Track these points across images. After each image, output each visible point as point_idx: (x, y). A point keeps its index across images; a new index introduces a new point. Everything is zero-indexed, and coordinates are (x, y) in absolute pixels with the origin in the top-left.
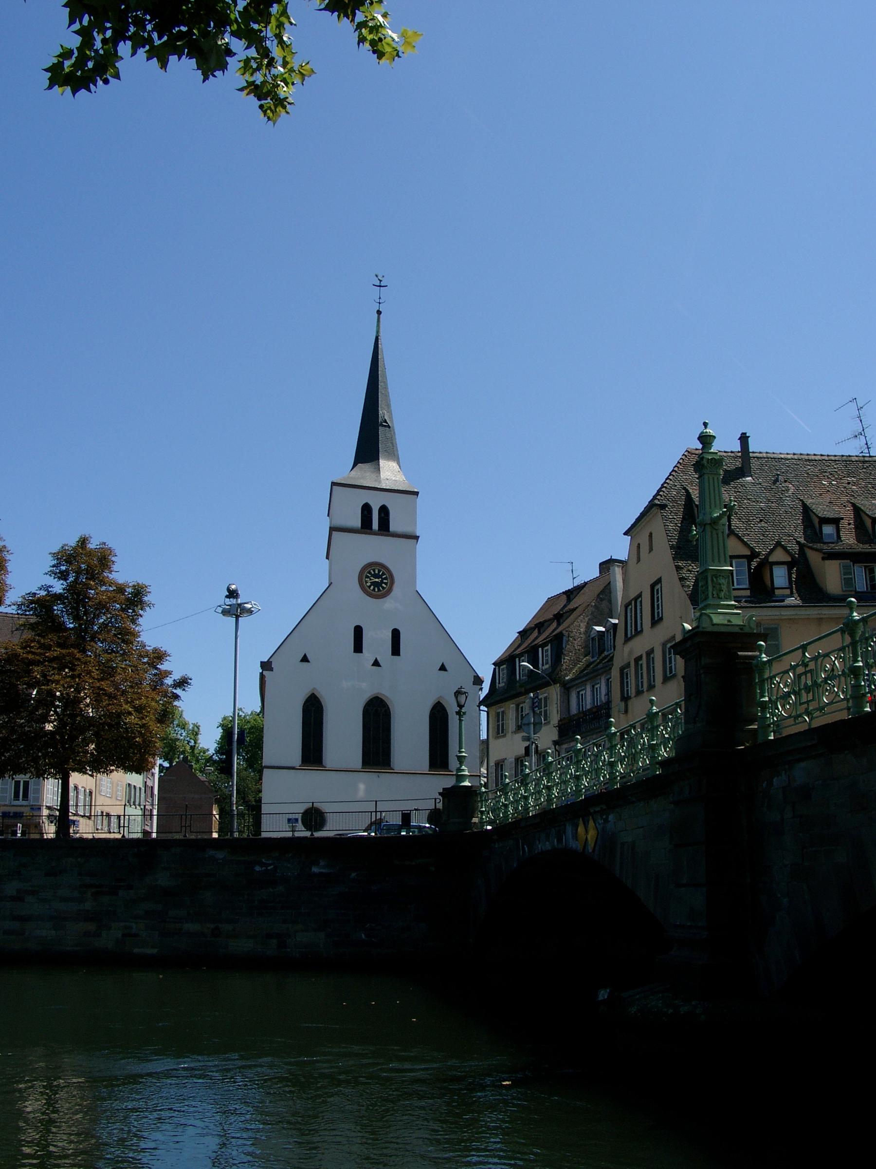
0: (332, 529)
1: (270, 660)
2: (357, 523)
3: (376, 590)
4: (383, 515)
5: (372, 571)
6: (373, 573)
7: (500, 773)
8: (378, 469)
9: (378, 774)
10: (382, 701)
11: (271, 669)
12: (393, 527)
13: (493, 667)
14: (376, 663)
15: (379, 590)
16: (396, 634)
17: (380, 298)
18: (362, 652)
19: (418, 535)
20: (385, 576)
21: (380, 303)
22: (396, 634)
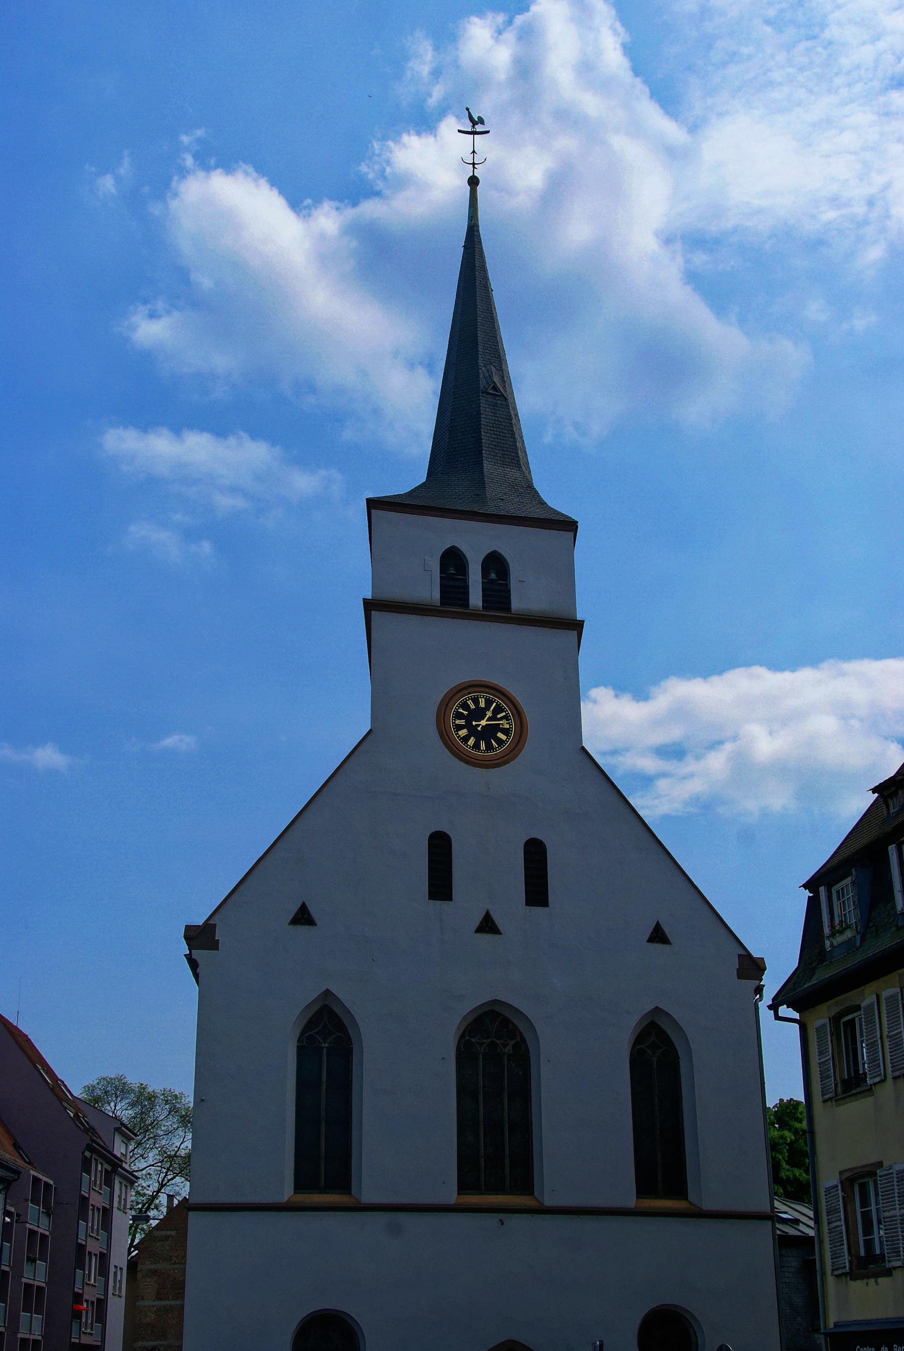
0: (370, 606)
1: (211, 922)
2: (432, 593)
3: (483, 746)
4: (493, 576)
6: (473, 706)
8: (480, 483)
9: (502, 1216)
10: (506, 1021)
11: (214, 945)
13: (807, 894)
14: (488, 926)
15: (489, 747)
18: (451, 900)
19: (579, 617)
20: (504, 714)
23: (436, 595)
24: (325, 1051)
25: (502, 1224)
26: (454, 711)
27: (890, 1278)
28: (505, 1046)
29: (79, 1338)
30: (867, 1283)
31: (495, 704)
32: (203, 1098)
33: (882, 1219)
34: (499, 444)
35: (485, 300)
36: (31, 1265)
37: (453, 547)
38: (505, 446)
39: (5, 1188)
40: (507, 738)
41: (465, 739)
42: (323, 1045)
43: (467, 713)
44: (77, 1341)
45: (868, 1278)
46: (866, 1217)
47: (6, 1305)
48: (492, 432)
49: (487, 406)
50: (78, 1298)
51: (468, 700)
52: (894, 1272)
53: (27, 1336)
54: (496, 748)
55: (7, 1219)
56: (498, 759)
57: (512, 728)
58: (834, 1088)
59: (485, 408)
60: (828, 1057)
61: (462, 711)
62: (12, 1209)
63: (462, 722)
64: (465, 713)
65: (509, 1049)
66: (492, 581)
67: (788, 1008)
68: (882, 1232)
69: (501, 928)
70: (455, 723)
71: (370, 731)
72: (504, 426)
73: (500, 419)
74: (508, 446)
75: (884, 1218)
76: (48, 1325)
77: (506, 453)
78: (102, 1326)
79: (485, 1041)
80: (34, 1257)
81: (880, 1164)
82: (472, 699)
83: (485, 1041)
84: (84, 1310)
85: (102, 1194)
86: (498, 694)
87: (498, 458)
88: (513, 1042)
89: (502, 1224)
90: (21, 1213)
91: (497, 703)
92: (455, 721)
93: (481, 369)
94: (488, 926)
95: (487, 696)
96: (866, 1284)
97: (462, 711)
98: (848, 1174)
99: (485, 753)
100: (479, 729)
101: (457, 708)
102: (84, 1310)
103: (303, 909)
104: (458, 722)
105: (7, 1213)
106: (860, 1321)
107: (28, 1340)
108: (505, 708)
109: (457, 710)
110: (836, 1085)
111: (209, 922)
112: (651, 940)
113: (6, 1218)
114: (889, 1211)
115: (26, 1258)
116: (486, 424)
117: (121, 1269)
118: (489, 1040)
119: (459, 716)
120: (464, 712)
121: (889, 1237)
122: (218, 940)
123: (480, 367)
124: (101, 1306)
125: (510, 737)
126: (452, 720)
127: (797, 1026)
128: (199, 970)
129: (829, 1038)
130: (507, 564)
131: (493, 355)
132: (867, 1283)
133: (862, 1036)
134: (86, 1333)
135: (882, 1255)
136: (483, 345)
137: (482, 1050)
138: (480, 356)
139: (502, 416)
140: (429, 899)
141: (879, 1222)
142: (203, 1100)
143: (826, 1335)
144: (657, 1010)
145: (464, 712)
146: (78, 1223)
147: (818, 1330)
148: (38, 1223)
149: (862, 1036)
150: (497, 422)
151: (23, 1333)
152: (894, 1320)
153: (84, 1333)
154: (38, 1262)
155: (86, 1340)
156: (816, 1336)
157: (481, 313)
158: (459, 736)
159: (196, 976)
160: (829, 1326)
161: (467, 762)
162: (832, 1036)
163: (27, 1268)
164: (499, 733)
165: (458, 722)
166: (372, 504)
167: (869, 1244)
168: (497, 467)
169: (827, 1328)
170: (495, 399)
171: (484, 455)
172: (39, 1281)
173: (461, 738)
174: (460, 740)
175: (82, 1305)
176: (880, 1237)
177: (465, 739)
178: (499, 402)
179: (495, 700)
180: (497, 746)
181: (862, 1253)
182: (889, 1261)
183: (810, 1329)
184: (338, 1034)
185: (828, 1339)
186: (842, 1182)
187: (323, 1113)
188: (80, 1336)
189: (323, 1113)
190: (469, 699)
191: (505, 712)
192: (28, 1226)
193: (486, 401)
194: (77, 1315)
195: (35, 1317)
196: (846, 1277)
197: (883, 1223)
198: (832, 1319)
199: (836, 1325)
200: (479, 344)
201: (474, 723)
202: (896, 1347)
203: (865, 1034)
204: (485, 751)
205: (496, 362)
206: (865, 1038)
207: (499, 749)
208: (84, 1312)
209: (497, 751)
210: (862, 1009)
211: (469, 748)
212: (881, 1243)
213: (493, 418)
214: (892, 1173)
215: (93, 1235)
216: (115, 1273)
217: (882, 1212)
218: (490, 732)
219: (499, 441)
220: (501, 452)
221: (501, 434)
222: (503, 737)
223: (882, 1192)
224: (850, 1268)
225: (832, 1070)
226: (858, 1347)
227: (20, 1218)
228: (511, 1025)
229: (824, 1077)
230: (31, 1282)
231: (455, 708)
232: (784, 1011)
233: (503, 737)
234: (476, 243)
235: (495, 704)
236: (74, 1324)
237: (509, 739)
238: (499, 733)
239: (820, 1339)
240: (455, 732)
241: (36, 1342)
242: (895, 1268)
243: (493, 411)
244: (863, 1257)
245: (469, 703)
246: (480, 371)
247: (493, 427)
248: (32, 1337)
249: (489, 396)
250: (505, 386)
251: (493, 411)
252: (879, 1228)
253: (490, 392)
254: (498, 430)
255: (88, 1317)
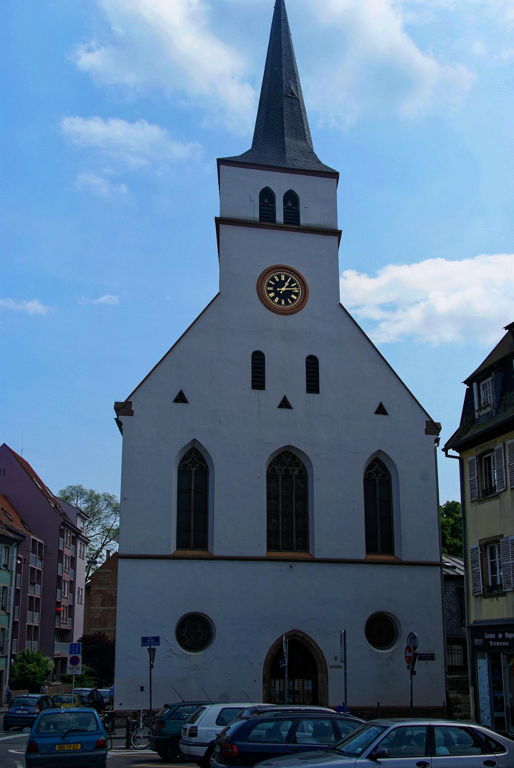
0: (219, 221)
2: (255, 214)
3: (283, 302)
4: (290, 204)
5: (276, 277)
6: (277, 280)
7: (489, 561)
8: (283, 150)
9: (291, 563)
10: (295, 457)
13: (466, 387)
14: (285, 404)
15: (287, 303)
20: (295, 284)
23: (257, 215)
24: (193, 472)
25: (291, 567)
26: (267, 282)
27: (505, 597)
28: (294, 471)
29: (60, 626)
30: (492, 600)
31: (290, 278)
32: (126, 497)
33: (502, 566)
34: (294, 127)
35: (287, 40)
36: (33, 586)
37: (267, 187)
38: (297, 128)
39: (17, 545)
40: (297, 298)
41: (273, 298)
42: (192, 469)
43: (274, 283)
44: (58, 627)
45: (493, 597)
46: (493, 564)
47: (21, 575)
48: (290, 120)
49: (287, 104)
50: (59, 604)
51: (275, 276)
52: (507, 594)
53: (31, 624)
54: (291, 303)
55: (19, 562)
56: (292, 310)
57: (300, 292)
58: (477, 495)
59: (286, 105)
60: (475, 478)
62: (22, 556)
63: (272, 289)
64: (273, 283)
65: (296, 472)
66: (289, 208)
67: (453, 450)
68: (501, 573)
69: (292, 406)
70: (267, 289)
71: (219, 293)
72: (297, 116)
73: (294, 112)
74: (300, 128)
75: (503, 565)
76: (44, 592)
77: (298, 132)
78: (72, 620)
79: (282, 468)
80: (34, 582)
81: (502, 536)
82: (277, 276)
83: (282, 468)
84: (62, 610)
85: (70, 549)
86: (292, 273)
87: (294, 135)
88: (298, 468)
89: (291, 567)
90: (26, 559)
91: (291, 278)
92: (267, 288)
93: (284, 82)
94: (285, 404)
95: (285, 274)
96: (491, 601)
97: (271, 282)
98: (484, 541)
99: (284, 306)
100: (281, 292)
101: (269, 280)
102: (62, 610)
103: (181, 394)
104: (269, 288)
105: (19, 558)
106: (488, 620)
107: (32, 626)
108: (296, 281)
109: (269, 281)
110: (479, 493)
111: (128, 401)
112: (377, 412)
113: (18, 561)
114: (506, 561)
115: (29, 583)
116: (286, 115)
117: (82, 589)
118: (286, 468)
119: (269, 285)
120: (273, 283)
121: (505, 575)
122: (133, 410)
123: (283, 81)
124: (71, 608)
125: (299, 297)
126: (266, 287)
127: (457, 461)
128: (122, 427)
129: (476, 467)
130: (298, 197)
131: (291, 74)
132: (492, 600)
133: (494, 466)
134: (63, 623)
135: (501, 585)
136: (285, 67)
137: (281, 473)
138: (283, 74)
139: (296, 110)
140: (252, 389)
141: (500, 568)
142: (125, 499)
143: (469, 627)
144: (379, 451)
145: (273, 283)
146: (58, 564)
147: (463, 625)
148: (36, 564)
149: (494, 466)
150: (293, 114)
151: (29, 622)
152: (506, 620)
153: (62, 623)
154: (36, 585)
155: (63, 627)
156: (463, 628)
157: (284, 48)
158: (270, 297)
159: (121, 430)
160: (470, 623)
161: (274, 312)
162: (477, 466)
163: (30, 588)
164: (292, 295)
165: (269, 288)
166: (221, 162)
167: (494, 579)
168: (293, 141)
169: (469, 624)
170: (292, 100)
171: (285, 133)
172: (37, 595)
173: (271, 298)
174: (270, 299)
175: (61, 608)
176: (500, 576)
177: (273, 298)
178: (294, 102)
179: (290, 276)
180: (291, 303)
181: (490, 584)
182: (505, 588)
183: (460, 624)
184: (201, 463)
185: (470, 630)
186: (480, 546)
187: (192, 506)
188: (60, 624)
189: (192, 506)
190: (275, 275)
191: (296, 283)
192: (30, 565)
193: (286, 101)
194: (58, 613)
195: (36, 614)
196: (481, 597)
197: (502, 568)
198: (473, 618)
199: (475, 622)
200: (283, 66)
201: (278, 289)
202: (506, 634)
203: (496, 465)
204: (284, 305)
205: (293, 78)
206: (496, 467)
207: (292, 304)
208: (62, 612)
209: (291, 305)
210: (495, 451)
211: (275, 304)
212: (501, 579)
213: (291, 111)
214: (508, 541)
215: (67, 546)
216: (79, 592)
217: (502, 562)
218: (287, 295)
219: (294, 125)
220: (295, 131)
221: (295, 121)
222: (295, 297)
223: (502, 551)
224: (483, 592)
225: (477, 485)
226: (486, 634)
227: (26, 561)
228: (297, 460)
229: (472, 488)
230: (33, 595)
231: (268, 281)
232: (451, 452)
233: (295, 297)
234: (282, 5)
235: (290, 278)
236: (56, 618)
237: (298, 299)
238: (292, 295)
239: (465, 630)
240: (267, 294)
241: (36, 627)
242: (508, 592)
243: (291, 107)
244: (490, 586)
245: (276, 278)
246: (283, 83)
247: (291, 117)
248: (34, 624)
249: (289, 98)
250: (298, 92)
251: (291, 107)
252: (500, 571)
253: (289, 95)
254: (294, 118)
255: (64, 614)
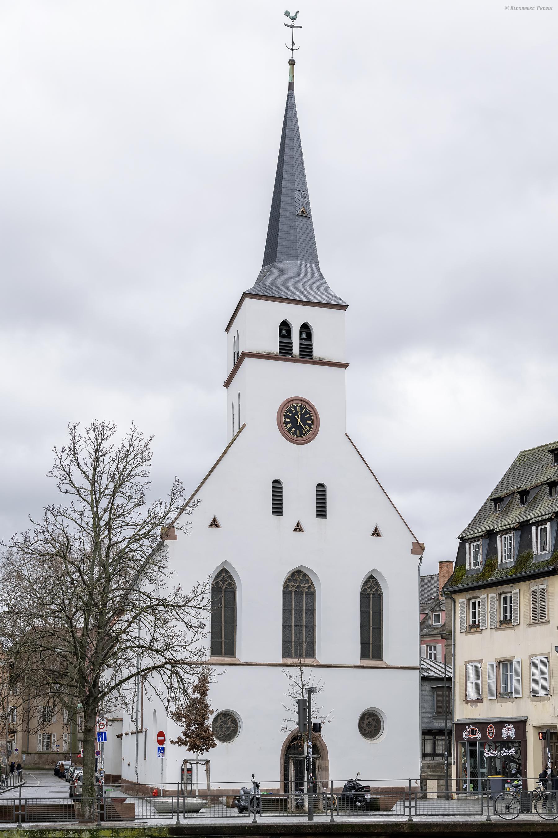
3: (298, 433)
6: (294, 411)
10: (305, 575)
12: (317, 353)
14: (298, 528)
16: (321, 490)
17: (293, 43)
20: (309, 415)
21: (292, 50)
22: (321, 490)
31: (304, 410)
61: (289, 414)
63: (288, 420)
70: (285, 420)
79: (295, 585)
83: (295, 585)
94: (298, 528)
97: (289, 414)
104: (287, 420)
120: (290, 414)
158: (287, 428)
165: (287, 420)
235: (304, 410)
